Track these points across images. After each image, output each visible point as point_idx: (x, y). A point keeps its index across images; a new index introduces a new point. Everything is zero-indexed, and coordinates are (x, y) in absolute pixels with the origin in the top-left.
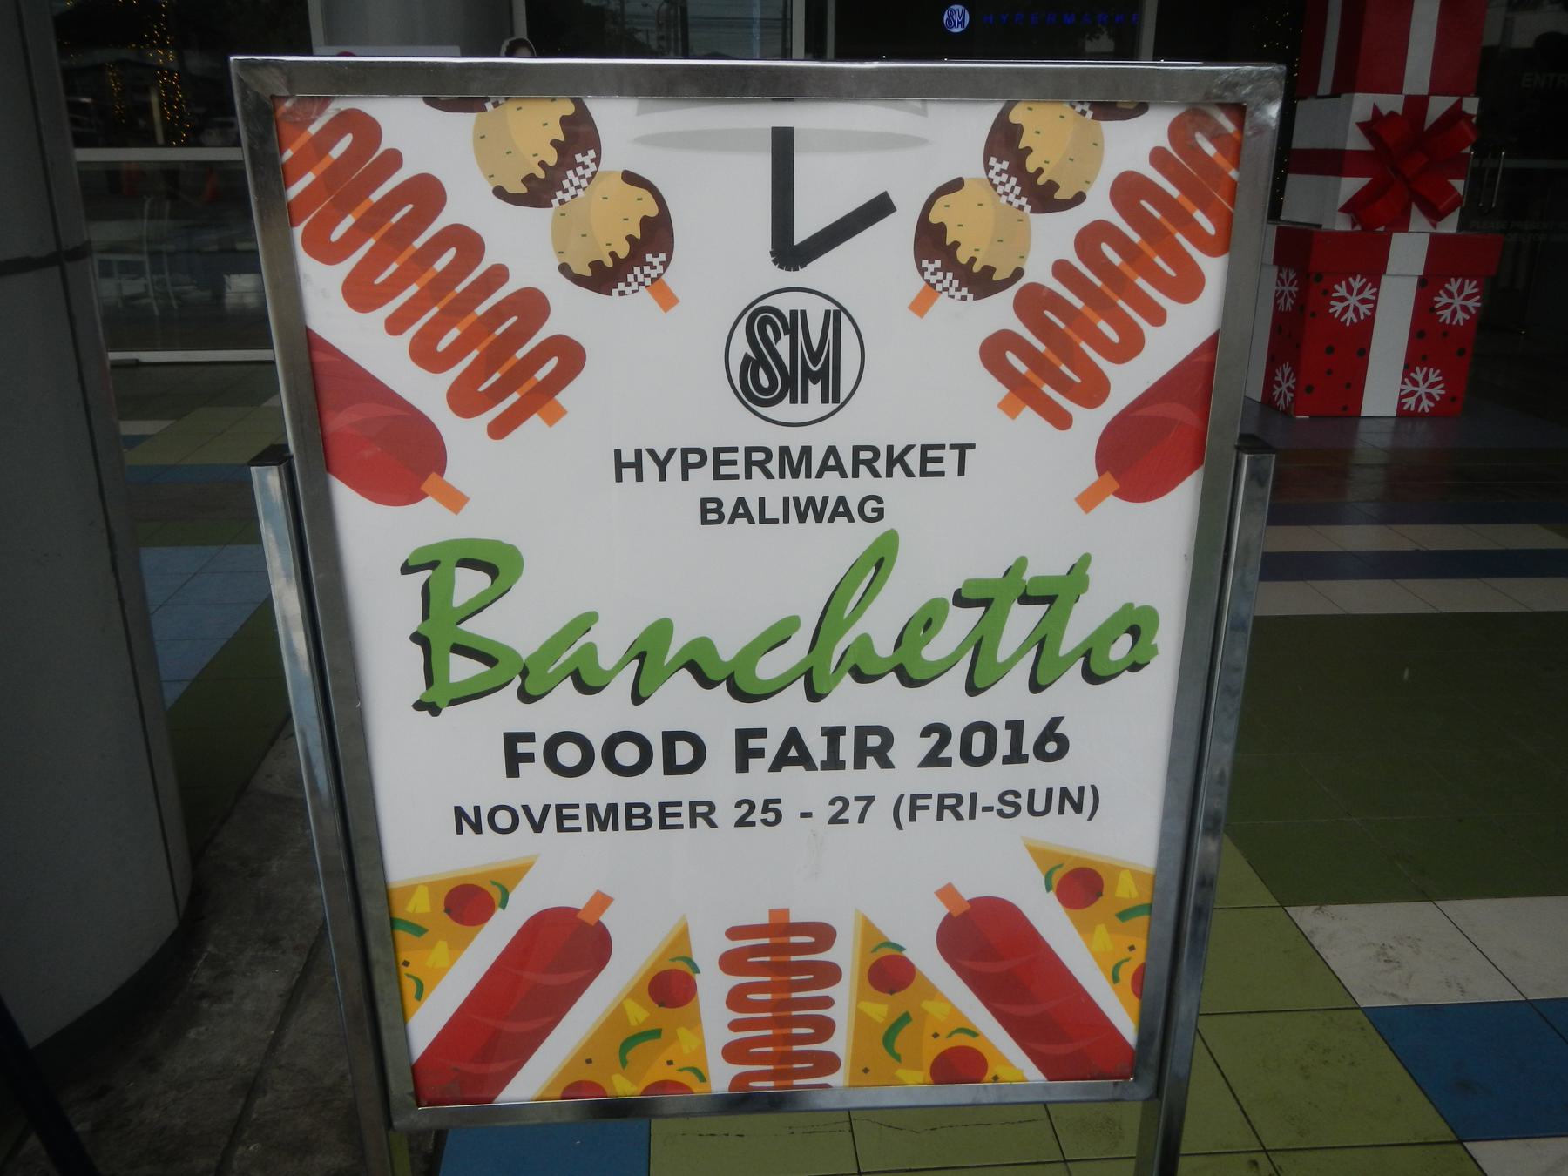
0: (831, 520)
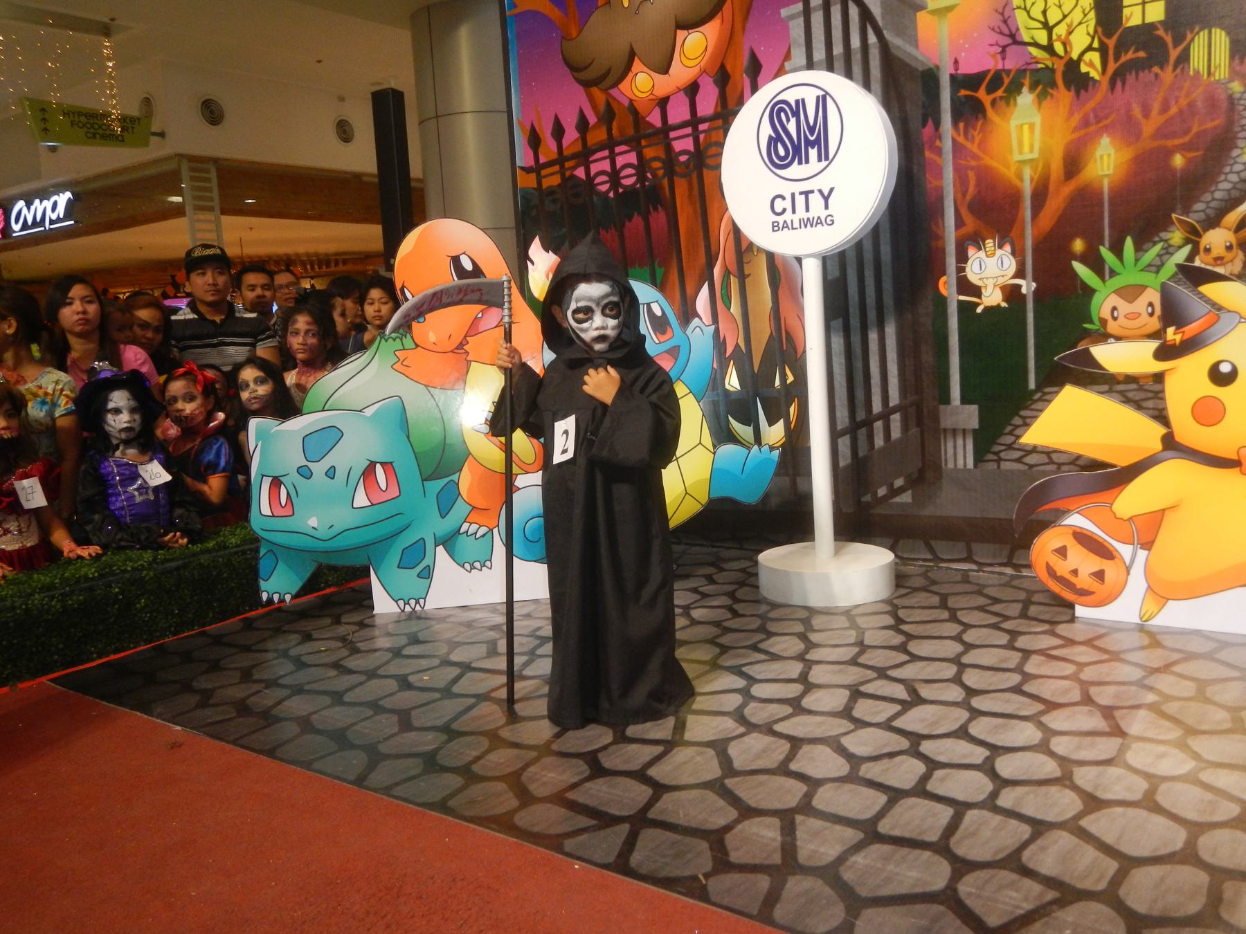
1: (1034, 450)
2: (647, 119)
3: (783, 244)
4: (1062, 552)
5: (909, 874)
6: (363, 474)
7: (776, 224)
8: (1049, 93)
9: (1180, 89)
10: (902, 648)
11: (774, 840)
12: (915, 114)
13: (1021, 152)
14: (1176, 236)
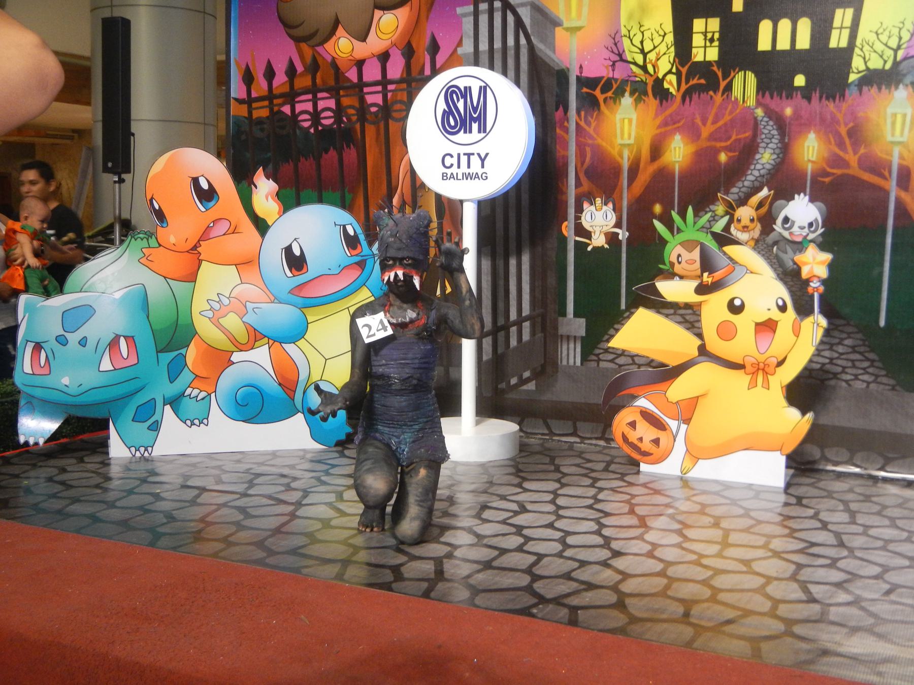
1: (623, 353)
2: (346, 75)
3: (450, 190)
4: (633, 425)
5: (507, 581)
6: (109, 344)
7: (445, 175)
8: (642, 99)
9: (726, 109)
10: (519, 485)
11: (431, 569)
12: (551, 101)
13: (622, 138)
14: (720, 209)
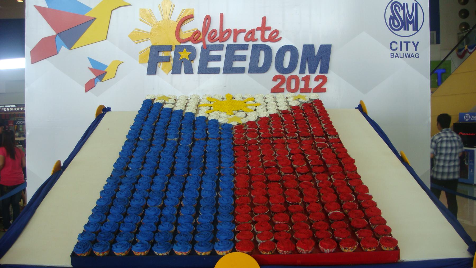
0: (411, 57)
7: (392, 54)
